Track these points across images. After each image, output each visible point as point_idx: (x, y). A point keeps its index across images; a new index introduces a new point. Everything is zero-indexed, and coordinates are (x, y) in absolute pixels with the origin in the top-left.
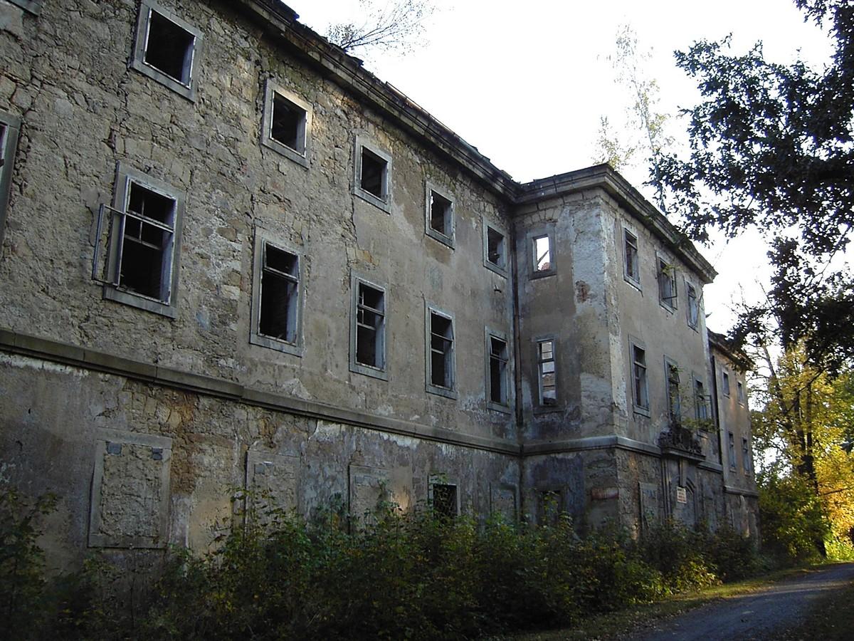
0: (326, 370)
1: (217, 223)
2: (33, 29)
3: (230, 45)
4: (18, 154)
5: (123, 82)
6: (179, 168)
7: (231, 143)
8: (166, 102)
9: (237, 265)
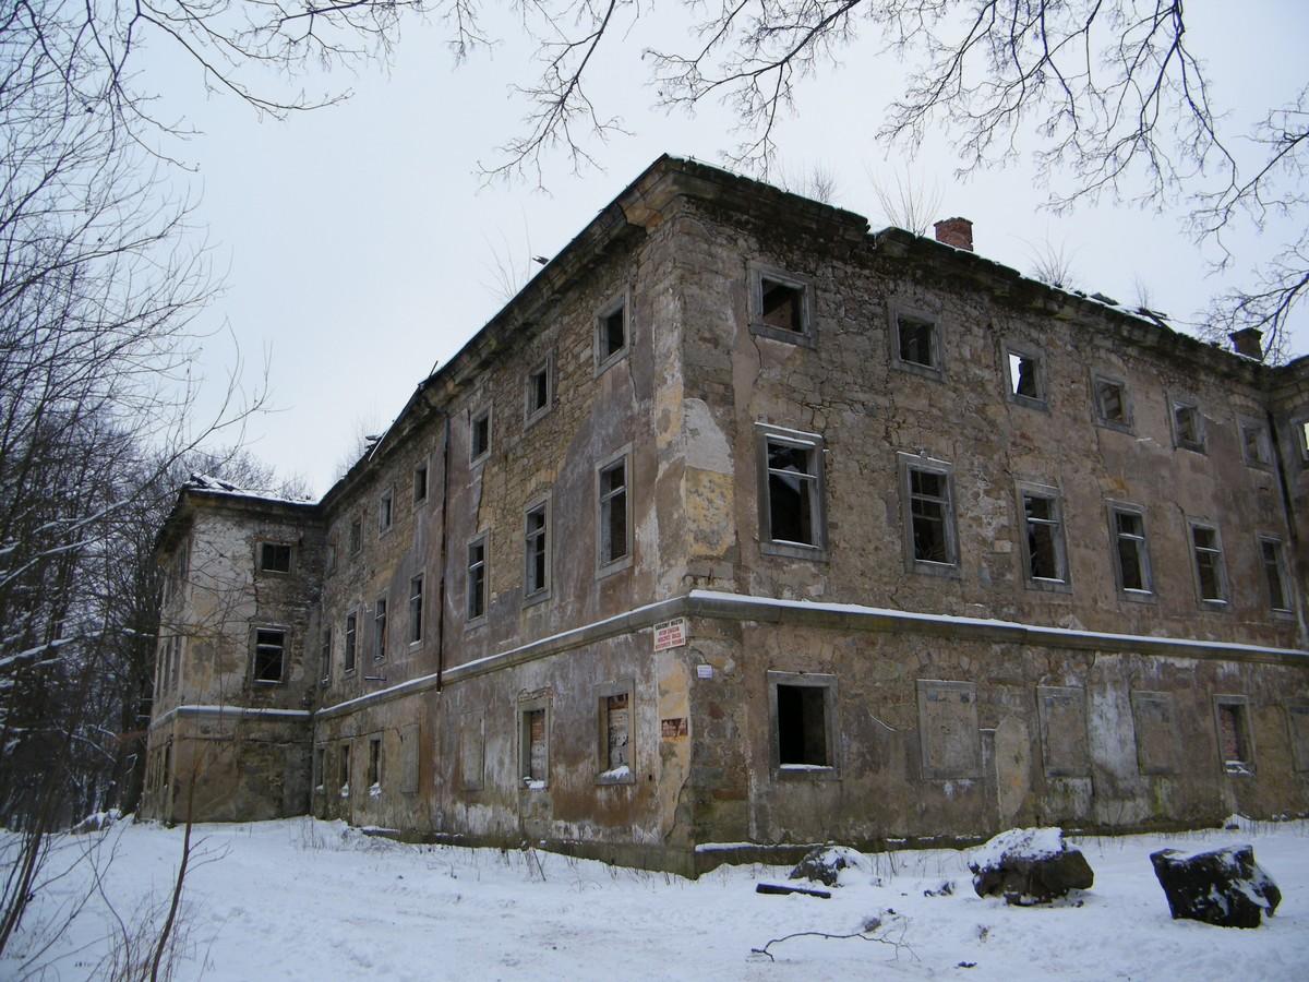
0: (1096, 603)
1: (981, 486)
2: (816, 360)
3: (964, 319)
4: (826, 467)
5: (887, 382)
6: (943, 444)
7: (981, 410)
8: (923, 389)
9: (1004, 520)
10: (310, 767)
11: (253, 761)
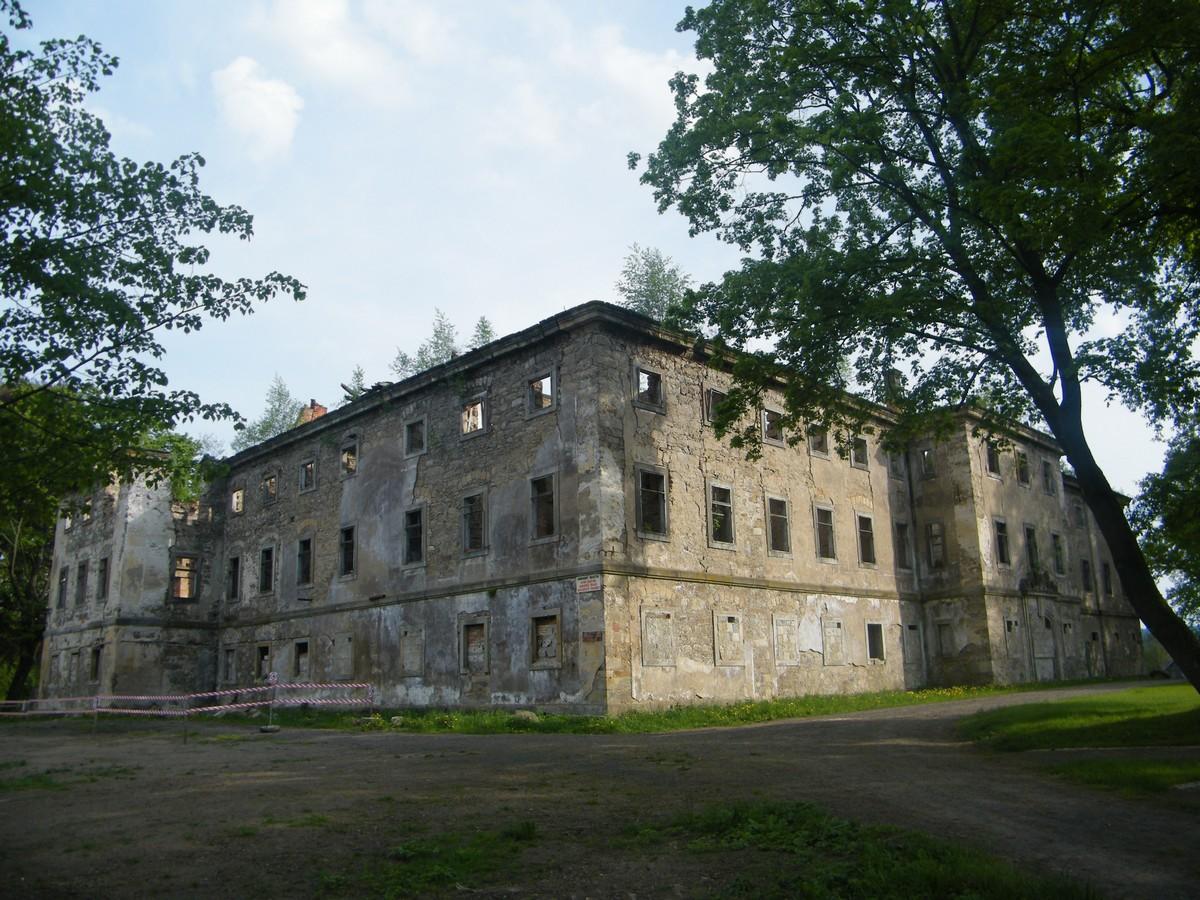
10: (216, 665)
11: (173, 659)
